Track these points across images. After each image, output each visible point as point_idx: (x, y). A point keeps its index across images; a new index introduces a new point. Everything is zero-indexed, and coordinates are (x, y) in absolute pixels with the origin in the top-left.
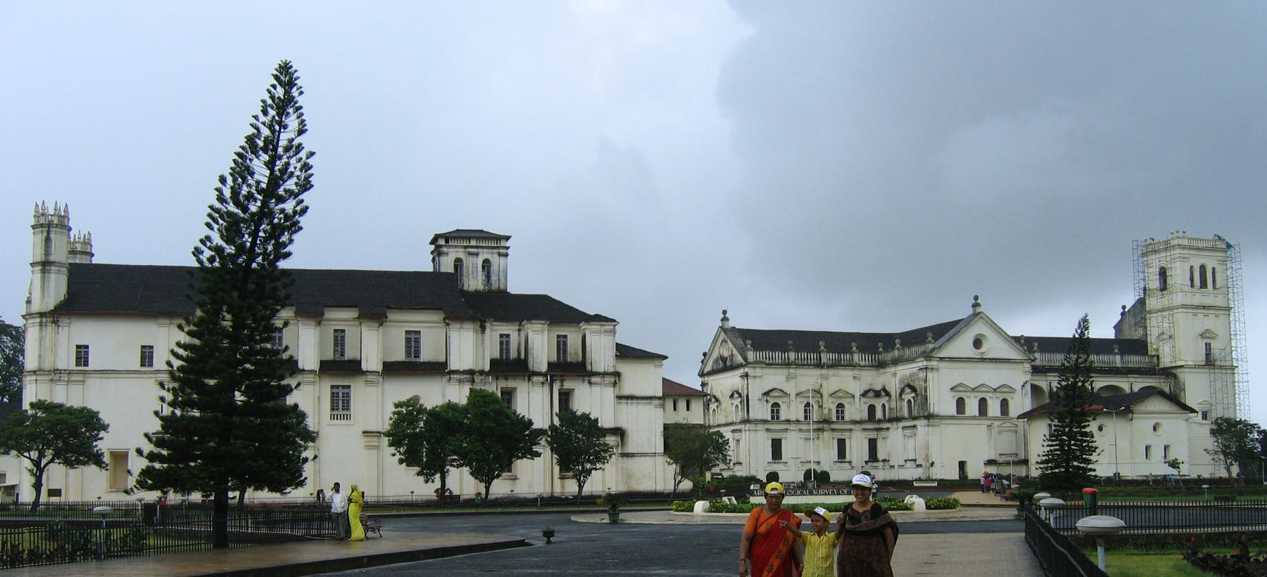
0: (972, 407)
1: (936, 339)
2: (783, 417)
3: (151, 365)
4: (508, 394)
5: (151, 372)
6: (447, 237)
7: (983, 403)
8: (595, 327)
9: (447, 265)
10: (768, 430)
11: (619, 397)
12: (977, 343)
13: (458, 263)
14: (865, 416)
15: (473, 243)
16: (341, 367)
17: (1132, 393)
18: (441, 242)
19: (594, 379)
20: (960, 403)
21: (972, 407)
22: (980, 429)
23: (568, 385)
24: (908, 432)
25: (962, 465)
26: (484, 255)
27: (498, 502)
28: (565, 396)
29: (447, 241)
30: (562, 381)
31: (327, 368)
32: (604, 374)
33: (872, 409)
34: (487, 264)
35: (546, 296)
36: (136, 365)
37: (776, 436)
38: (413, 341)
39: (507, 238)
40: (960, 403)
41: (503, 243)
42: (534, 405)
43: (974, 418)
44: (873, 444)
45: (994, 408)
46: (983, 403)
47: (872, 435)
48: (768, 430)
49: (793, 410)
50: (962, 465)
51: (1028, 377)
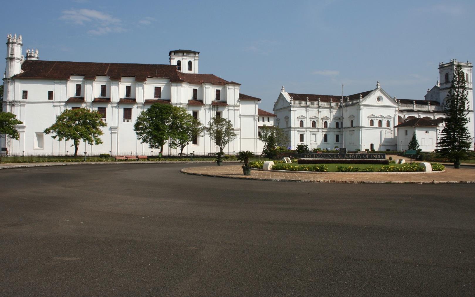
0: (376, 124)
1: (363, 97)
2: (305, 126)
3: (52, 99)
4: (195, 114)
5: (53, 102)
6: (175, 52)
7: (380, 122)
8: (231, 87)
9: (174, 62)
10: (298, 131)
11: (240, 116)
12: (379, 99)
13: (179, 63)
14: (335, 127)
15: (185, 54)
16: (128, 101)
17: (435, 120)
18: (173, 54)
19: (230, 108)
20: (372, 122)
21: (376, 124)
22: (377, 132)
23: (220, 109)
24: (351, 132)
25: (372, 145)
26: (189, 59)
27: (193, 157)
28: (218, 114)
29: (175, 54)
30: (217, 108)
31: (121, 102)
32: (234, 106)
33: (337, 124)
34: (190, 63)
35: (212, 75)
36: (46, 99)
37: (302, 133)
38: (157, 90)
39: (198, 53)
40: (372, 122)
41: (197, 55)
42: (206, 117)
43: (377, 128)
44: (337, 137)
45: (384, 124)
46: (380, 122)
47: (338, 133)
48: (298, 131)
49: (308, 123)
50: (372, 145)
51: (397, 112)
